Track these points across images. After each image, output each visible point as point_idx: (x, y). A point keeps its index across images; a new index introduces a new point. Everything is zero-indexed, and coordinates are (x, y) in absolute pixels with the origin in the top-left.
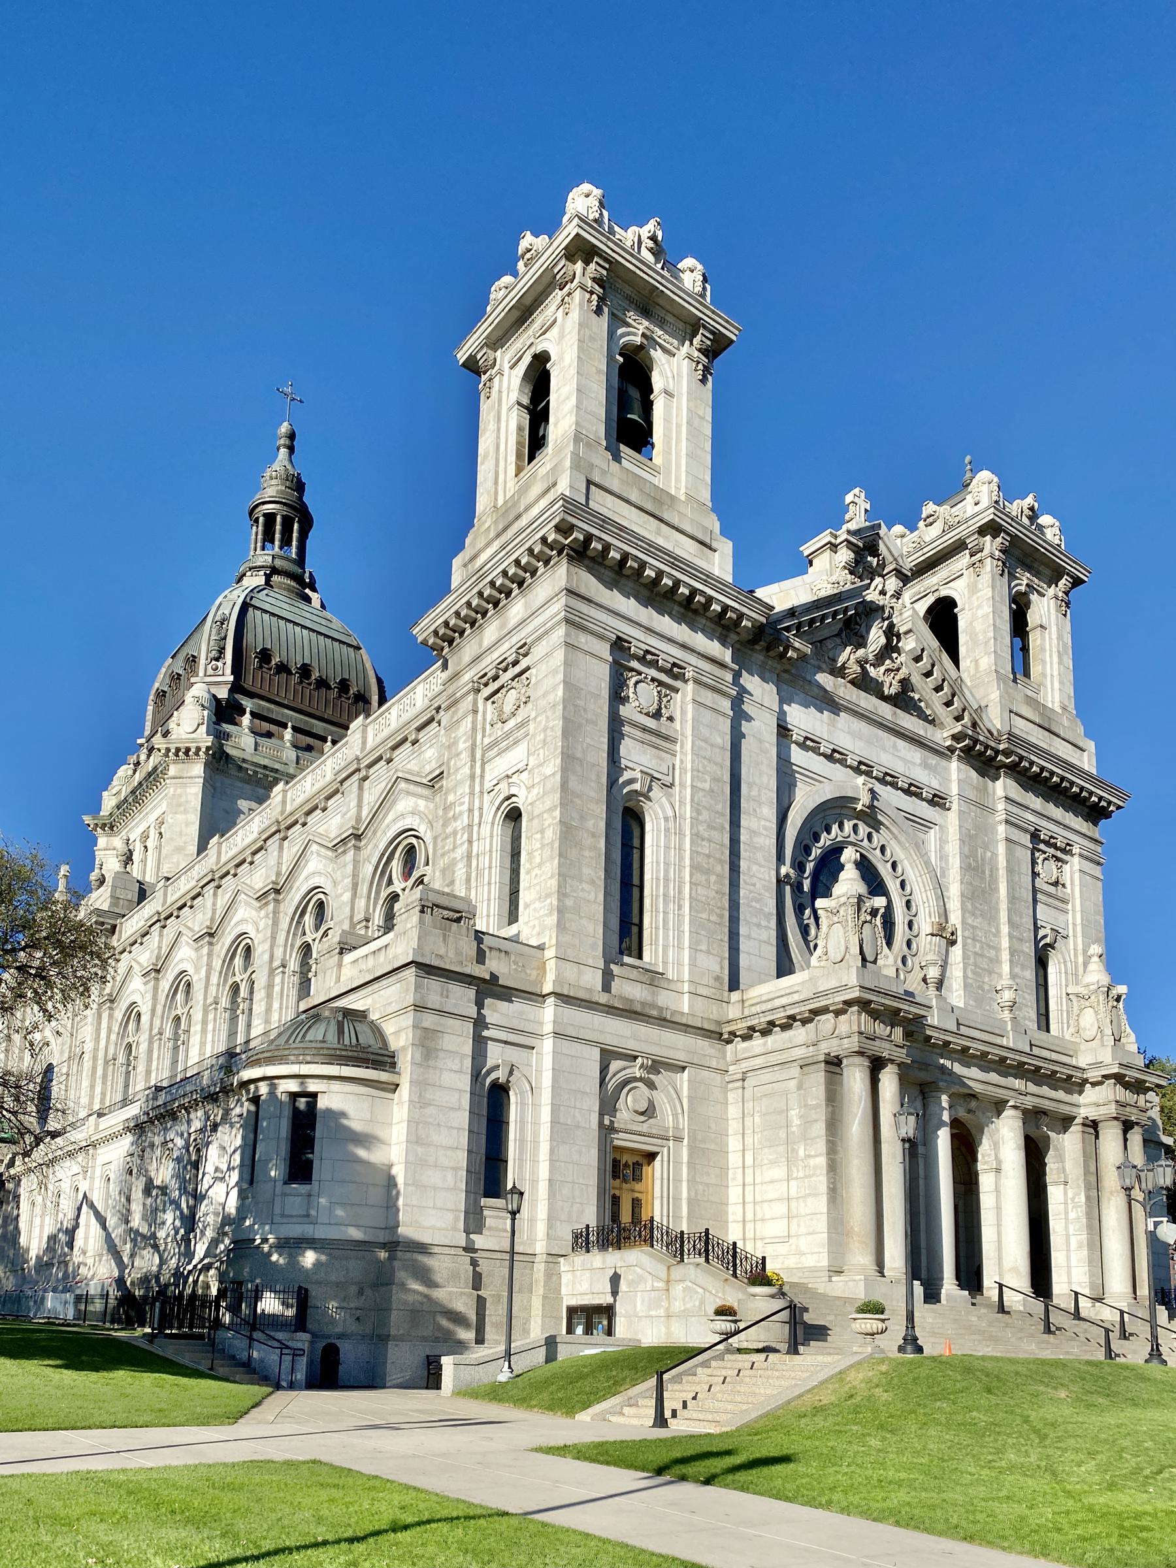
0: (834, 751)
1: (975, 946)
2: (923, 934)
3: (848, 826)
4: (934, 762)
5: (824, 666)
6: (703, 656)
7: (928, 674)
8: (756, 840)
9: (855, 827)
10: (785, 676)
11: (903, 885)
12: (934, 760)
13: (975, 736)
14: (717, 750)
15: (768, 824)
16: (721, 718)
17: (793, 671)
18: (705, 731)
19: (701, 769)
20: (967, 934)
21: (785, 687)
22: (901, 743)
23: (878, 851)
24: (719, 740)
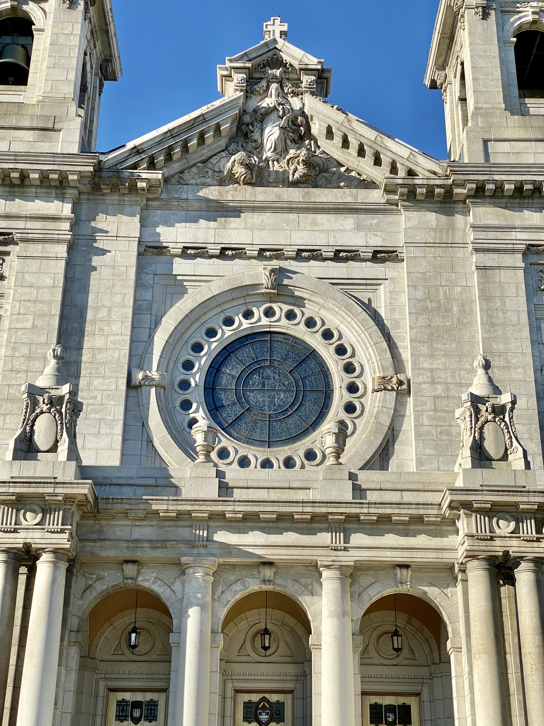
0: (224, 249)
1: (436, 391)
2: (370, 390)
3: (259, 312)
4: (375, 222)
5: (209, 180)
6: (31, 218)
7: (346, 143)
8: (99, 357)
9: (269, 313)
10: (155, 203)
11: (341, 350)
12: (372, 220)
13: (410, 182)
14: (46, 290)
15: (118, 338)
16: (52, 263)
17: (164, 196)
18: (30, 279)
19: (22, 311)
20: (420, 379)
21: (159, 212)
22: (322, 218)
23: (302, 326)
24: (49, 282)
